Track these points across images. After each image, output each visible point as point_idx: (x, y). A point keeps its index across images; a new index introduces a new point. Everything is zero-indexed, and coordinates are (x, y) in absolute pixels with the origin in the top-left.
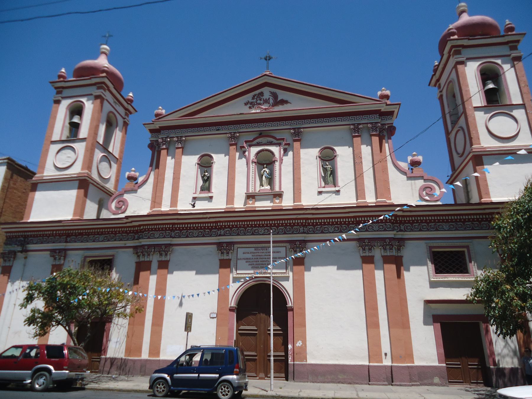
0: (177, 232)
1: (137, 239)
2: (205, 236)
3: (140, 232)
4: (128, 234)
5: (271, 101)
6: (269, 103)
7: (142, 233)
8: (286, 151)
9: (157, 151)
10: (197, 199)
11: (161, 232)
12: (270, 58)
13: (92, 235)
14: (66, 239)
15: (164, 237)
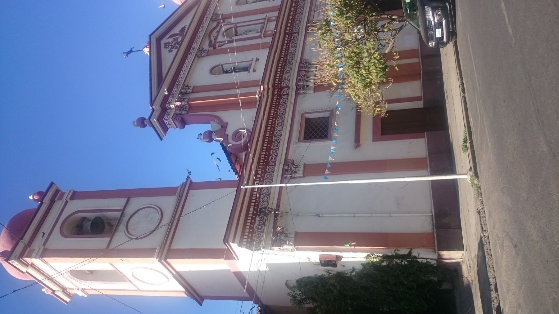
0: (287, 62)
1: (288, 96)
2: (296, 42)
3: (280, 92)
4: (279, 104)
5: (177, 37)
6: (179, 38)
7: (282, 91)
8: (229, 22)
9: (188, 113)
10: (255, 69)
11: (285, 73)
12: (131, 51)
13: (272, 138)
14: (271, 165)
15: (291, 69)
